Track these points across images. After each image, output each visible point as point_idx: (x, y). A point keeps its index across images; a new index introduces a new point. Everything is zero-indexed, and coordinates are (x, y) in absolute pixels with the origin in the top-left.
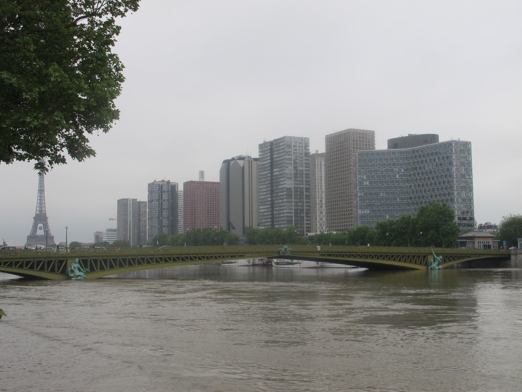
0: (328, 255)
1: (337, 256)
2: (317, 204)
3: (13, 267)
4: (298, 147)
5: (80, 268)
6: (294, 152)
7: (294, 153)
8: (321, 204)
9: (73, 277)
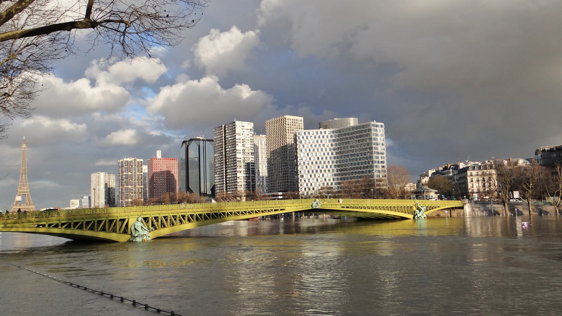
0: (275, 210)
2: (256, 173)
3: (72, 228)
4: (245, 129)
5: (143, 226)
6: (243, 133)
7: (242, 134)
9: (137, 237)
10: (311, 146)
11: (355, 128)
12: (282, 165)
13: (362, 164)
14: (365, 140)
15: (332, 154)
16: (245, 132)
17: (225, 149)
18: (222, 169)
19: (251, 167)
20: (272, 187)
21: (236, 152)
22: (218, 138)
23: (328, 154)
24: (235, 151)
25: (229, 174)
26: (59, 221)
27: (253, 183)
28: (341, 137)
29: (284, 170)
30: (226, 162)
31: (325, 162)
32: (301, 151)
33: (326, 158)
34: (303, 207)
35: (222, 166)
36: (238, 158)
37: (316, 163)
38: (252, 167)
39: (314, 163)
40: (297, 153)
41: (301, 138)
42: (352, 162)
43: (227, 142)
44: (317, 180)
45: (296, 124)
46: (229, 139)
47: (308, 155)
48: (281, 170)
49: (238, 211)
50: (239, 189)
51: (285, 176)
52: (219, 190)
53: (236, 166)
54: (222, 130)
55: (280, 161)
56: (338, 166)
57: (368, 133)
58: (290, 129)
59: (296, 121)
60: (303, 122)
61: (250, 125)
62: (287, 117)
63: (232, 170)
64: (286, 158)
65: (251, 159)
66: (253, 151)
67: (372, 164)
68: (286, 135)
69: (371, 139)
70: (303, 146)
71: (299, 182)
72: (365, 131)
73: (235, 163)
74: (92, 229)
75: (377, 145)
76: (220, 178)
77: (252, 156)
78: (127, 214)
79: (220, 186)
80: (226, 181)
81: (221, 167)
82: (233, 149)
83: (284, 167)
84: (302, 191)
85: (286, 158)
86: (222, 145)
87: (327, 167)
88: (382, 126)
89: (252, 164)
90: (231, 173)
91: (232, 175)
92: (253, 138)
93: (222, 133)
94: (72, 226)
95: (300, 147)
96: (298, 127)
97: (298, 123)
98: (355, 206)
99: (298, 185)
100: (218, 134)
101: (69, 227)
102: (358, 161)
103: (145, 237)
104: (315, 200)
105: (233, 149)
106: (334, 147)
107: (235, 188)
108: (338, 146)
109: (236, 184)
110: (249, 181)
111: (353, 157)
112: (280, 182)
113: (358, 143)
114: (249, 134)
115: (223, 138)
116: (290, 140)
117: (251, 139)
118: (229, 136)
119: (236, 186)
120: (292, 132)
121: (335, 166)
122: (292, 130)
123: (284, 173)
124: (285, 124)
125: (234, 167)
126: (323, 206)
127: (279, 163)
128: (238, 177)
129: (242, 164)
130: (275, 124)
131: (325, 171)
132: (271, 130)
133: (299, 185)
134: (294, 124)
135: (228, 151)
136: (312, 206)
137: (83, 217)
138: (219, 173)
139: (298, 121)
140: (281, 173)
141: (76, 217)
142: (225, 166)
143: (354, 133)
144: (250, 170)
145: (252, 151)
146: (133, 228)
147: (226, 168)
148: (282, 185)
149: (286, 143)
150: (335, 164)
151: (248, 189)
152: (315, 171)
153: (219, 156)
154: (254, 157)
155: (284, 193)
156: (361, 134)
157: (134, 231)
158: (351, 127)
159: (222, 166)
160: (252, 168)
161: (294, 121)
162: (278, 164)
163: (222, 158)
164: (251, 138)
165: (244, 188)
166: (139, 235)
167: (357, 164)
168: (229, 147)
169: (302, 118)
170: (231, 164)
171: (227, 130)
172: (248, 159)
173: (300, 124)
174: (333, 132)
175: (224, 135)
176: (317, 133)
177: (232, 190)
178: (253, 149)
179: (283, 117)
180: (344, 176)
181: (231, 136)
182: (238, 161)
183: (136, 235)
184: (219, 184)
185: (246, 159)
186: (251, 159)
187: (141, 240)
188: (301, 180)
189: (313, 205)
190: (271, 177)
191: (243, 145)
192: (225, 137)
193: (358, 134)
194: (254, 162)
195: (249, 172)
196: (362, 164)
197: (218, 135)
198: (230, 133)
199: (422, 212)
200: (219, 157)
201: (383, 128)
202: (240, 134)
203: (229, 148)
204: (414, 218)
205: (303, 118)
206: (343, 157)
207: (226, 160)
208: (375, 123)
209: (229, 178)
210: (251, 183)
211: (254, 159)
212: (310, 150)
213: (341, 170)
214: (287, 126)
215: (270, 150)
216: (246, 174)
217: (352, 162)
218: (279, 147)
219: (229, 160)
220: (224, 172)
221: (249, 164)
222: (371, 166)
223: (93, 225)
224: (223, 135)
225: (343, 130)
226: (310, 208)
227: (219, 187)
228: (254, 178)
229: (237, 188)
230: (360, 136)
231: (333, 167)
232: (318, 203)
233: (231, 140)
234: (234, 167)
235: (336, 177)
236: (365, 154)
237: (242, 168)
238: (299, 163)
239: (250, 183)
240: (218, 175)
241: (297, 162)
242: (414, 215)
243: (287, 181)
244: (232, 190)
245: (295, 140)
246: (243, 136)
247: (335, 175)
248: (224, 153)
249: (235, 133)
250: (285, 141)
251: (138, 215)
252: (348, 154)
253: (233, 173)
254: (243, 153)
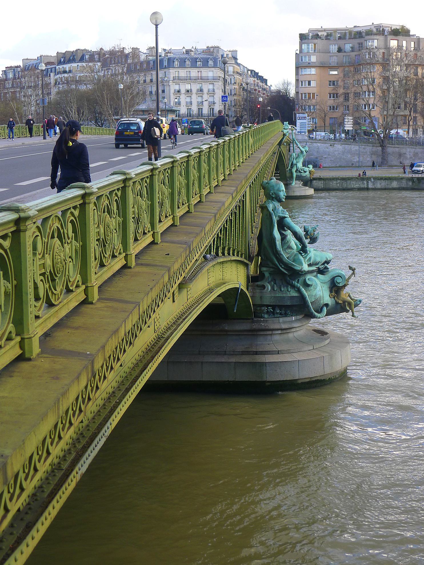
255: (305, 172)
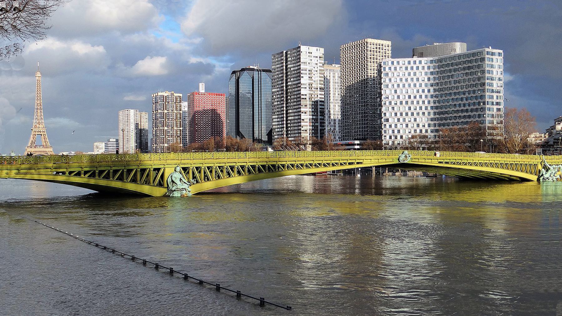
0: (350, 164)
1: (454, 164)
3: (97, 177)
4: (313, 57)
6: (310, 62)
7: (309, 63)
8: (330, 115)
9: (175, 191)
10: (401, 80)
11: (462, 57)
12: (361, 105)
13: (469, 106)
14: (475, 73)
15: (429, 91)
16: (313, 60)
17: (287, 83)
18: (282, 109)
19: (319, 107)
20: (346, 133)
21: (300, 86)
22: (278, 68)
23: (423, 91)
24: (299, 85)
25: (291, 115)
26: (82, 168)
27: (321, 128)
28: (442, 69)
29: (363, 112)
30: (287, 100)
31: (418, 102)
32: (387, 86)
33: (421, 97)
34: (387, 160)
35: (282, 104)
36: (303, 95)
37: (407, 103)
38: (321, 107)
39: (404, 102)
40: (381, 89)
41: (387, 69)
42: (455, 103)
43: (289, 73)
44: (407, 126)
45: (381, 50)
46: (292, 69)
47: (396, 91)
48: (359, 112)
49: (301, 162)
50: (303, 135)
51: (365, 119)
52: (278, 135)
53: (300, 104)
54: (282, 58)
55: (358, 99)
56: (437, 108)
57: (480, 63)
58: (372, 57)
59: (381, 47)
60: (390, 48)
61: (321, 51)
62: (369, 40)
63: (295, 111)
64: (366, 96)
65: (319, 96)
66: (323, 86)
67: (484, 106)
68: (367, 64)
69: (483, 72)
70: (390, 80)
71: (383, 127)
72: (476, 61)
73: (298, 101)
74: (121, 179)
75: (491, 80)
76: (278, 120)
77: (321, 93)
78: (163, 162)
79: (278, 130)
80: (287, 124)
81: (280, 106)
82: (297, 82)
83: (363, 108)
84: (386, 139)
85: (366, 96)
86: (283, 76)
87: (421, 108)
88: (500, 54)
89: (321, 103)
90: (293, 114)
91: (294, 116)
92: (323, 69)
93: (282, 61)
94: (97, 174)
95: (385, 80)
96: (384, 54)
97: (384, 49)
98: (457, 161)
99: (381, 132)
100: (277, 63)
101: (93, 175)
102: (465, 101)
103: (184, 192)
104: (403, 152)
105: (297, 82)
106: (432, 81)
107: (299, 133)
108: (437, 81)
109: (300, 128)
110: (316, 124)
111: (458, 96)
112: (357, 127)
113: (465, 77)
114: (318, 62)
115: (284, 67)
116: (372, 72)
117: (320, 70)
118: (292, 66)
119: (299, 131)
120: (375, 60)
121: (432, 108)
122: (375, 59)
123: (363, 115)
124: (367, 50)
125: (297, 107)
126: (413, 160)
127: (357, 102)
128: (302, 120)
129: (308, 103)
130: (353, 50)
131: (418, 114)
132: (348, 58)
133: (383, 131)
134: (378, 50)
135: (290, 85)
136: (399, 159)
137: (110, 163)
138: (278, 113)
139: (384, 47)
140: (358, 115)
141: (101, 164)
142: (286, 105)
143: (460, 63)
144: (317, 110)
145: (320, 86)
146: (170, 180)
147: (286, 107)
148: (360, 131)
149: (367, 75)
150: (432, 104)
151: (315, 135)
152: (404, 114)
153: (278, 91)
154: (323, 93)
155: (363, 141)
156: (470, 65)
157: (171, 184)
158: (457, 54)
159: (282, 104)
160: (320, 108)
161: (378, 46)
162: (356, 103)
163: (282, 94)
164: (321, 68)
165: (310, 134)
166: (177, 189)
167: (462, 105)
168: (292, 80)
169: (389, 43)
170: (294, 102)
171: (289, 57)
172: (316, 96)
173: (387, 51)
174: (431, 62)
175: (286, 64)
176: (409, 63)
177: (294, 135)
178: (322, 82)
179: (364, 41)
180: (444, 121)
181: (294, 65)
182: (302, 98)
183: (173, 189)
184: (278, 128)
185: (313, 96)
186: (319, 96)
187: (179, 195)
188: (385, 125)
189: (401, 159)
190: (345, 120)
191: (309, 77)
192: (286, 66)
193: (465, 65)
194: (323, 100)
195: (317, 113)
196: (469, 106)
197: (277, 64)
198: (293, 62)
199: (549, 172)
200: (278, 93)
201: (502, 58)
202: (306, 63)
203: (291, 81)
204: (538, 180)
205: (390, 42)
206: (444, 96)
207: (287, 97)
208: (490, 49)
209: (291, 120)
210: (319, 128)
211: (323, 96)
212: (398, 85)
213: (439, 113)
214: (369, 53)
215: (346, 85)
216: (313, 115)
217: (455, 103)
218: (357, 81)
219: (291, 97)
220: (285, 112)
221: (317, 103)
222: (482, 108)
223: (122, 174)
224: (284, 64)
225: (445, 59)
226: (396, 162)
227: (278, 132)
228: (323, 121)
229: (300, 133)
230: (469, 68)
231: (429, 108)
232: (407, 155)
233: (294, 70)
234: (297, 107)
235: (432, 123)
236: (474, 92)
237: (308, 108)
238: (383, 103)
239: (318, 128)
240: (276, 117)
241: (381, 101)
242: (539, 175)
243: (366, 126)
244: (294, 135)
245: (380, 72)
246: (310, 65)
247: (432, 120)
248: (285, 88)
249: (300, 61)
250: (366, 73)
251: (176, 164)
252: (451, 91)
253: (296, 114)
254: (309, 88)
255: (549, 179)
